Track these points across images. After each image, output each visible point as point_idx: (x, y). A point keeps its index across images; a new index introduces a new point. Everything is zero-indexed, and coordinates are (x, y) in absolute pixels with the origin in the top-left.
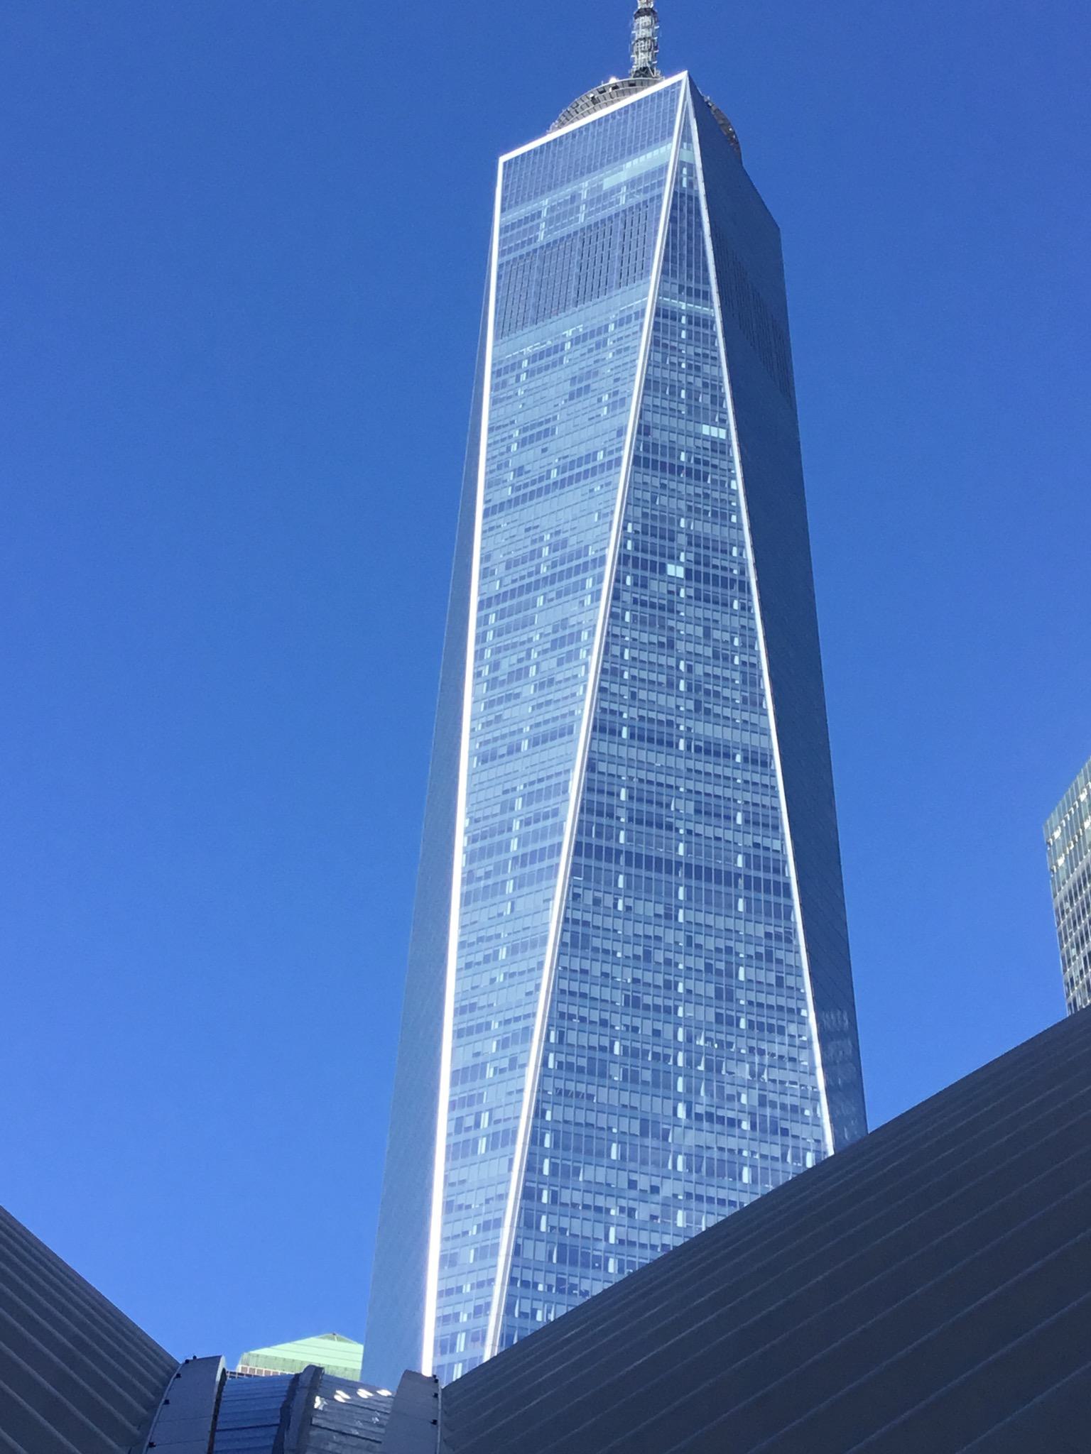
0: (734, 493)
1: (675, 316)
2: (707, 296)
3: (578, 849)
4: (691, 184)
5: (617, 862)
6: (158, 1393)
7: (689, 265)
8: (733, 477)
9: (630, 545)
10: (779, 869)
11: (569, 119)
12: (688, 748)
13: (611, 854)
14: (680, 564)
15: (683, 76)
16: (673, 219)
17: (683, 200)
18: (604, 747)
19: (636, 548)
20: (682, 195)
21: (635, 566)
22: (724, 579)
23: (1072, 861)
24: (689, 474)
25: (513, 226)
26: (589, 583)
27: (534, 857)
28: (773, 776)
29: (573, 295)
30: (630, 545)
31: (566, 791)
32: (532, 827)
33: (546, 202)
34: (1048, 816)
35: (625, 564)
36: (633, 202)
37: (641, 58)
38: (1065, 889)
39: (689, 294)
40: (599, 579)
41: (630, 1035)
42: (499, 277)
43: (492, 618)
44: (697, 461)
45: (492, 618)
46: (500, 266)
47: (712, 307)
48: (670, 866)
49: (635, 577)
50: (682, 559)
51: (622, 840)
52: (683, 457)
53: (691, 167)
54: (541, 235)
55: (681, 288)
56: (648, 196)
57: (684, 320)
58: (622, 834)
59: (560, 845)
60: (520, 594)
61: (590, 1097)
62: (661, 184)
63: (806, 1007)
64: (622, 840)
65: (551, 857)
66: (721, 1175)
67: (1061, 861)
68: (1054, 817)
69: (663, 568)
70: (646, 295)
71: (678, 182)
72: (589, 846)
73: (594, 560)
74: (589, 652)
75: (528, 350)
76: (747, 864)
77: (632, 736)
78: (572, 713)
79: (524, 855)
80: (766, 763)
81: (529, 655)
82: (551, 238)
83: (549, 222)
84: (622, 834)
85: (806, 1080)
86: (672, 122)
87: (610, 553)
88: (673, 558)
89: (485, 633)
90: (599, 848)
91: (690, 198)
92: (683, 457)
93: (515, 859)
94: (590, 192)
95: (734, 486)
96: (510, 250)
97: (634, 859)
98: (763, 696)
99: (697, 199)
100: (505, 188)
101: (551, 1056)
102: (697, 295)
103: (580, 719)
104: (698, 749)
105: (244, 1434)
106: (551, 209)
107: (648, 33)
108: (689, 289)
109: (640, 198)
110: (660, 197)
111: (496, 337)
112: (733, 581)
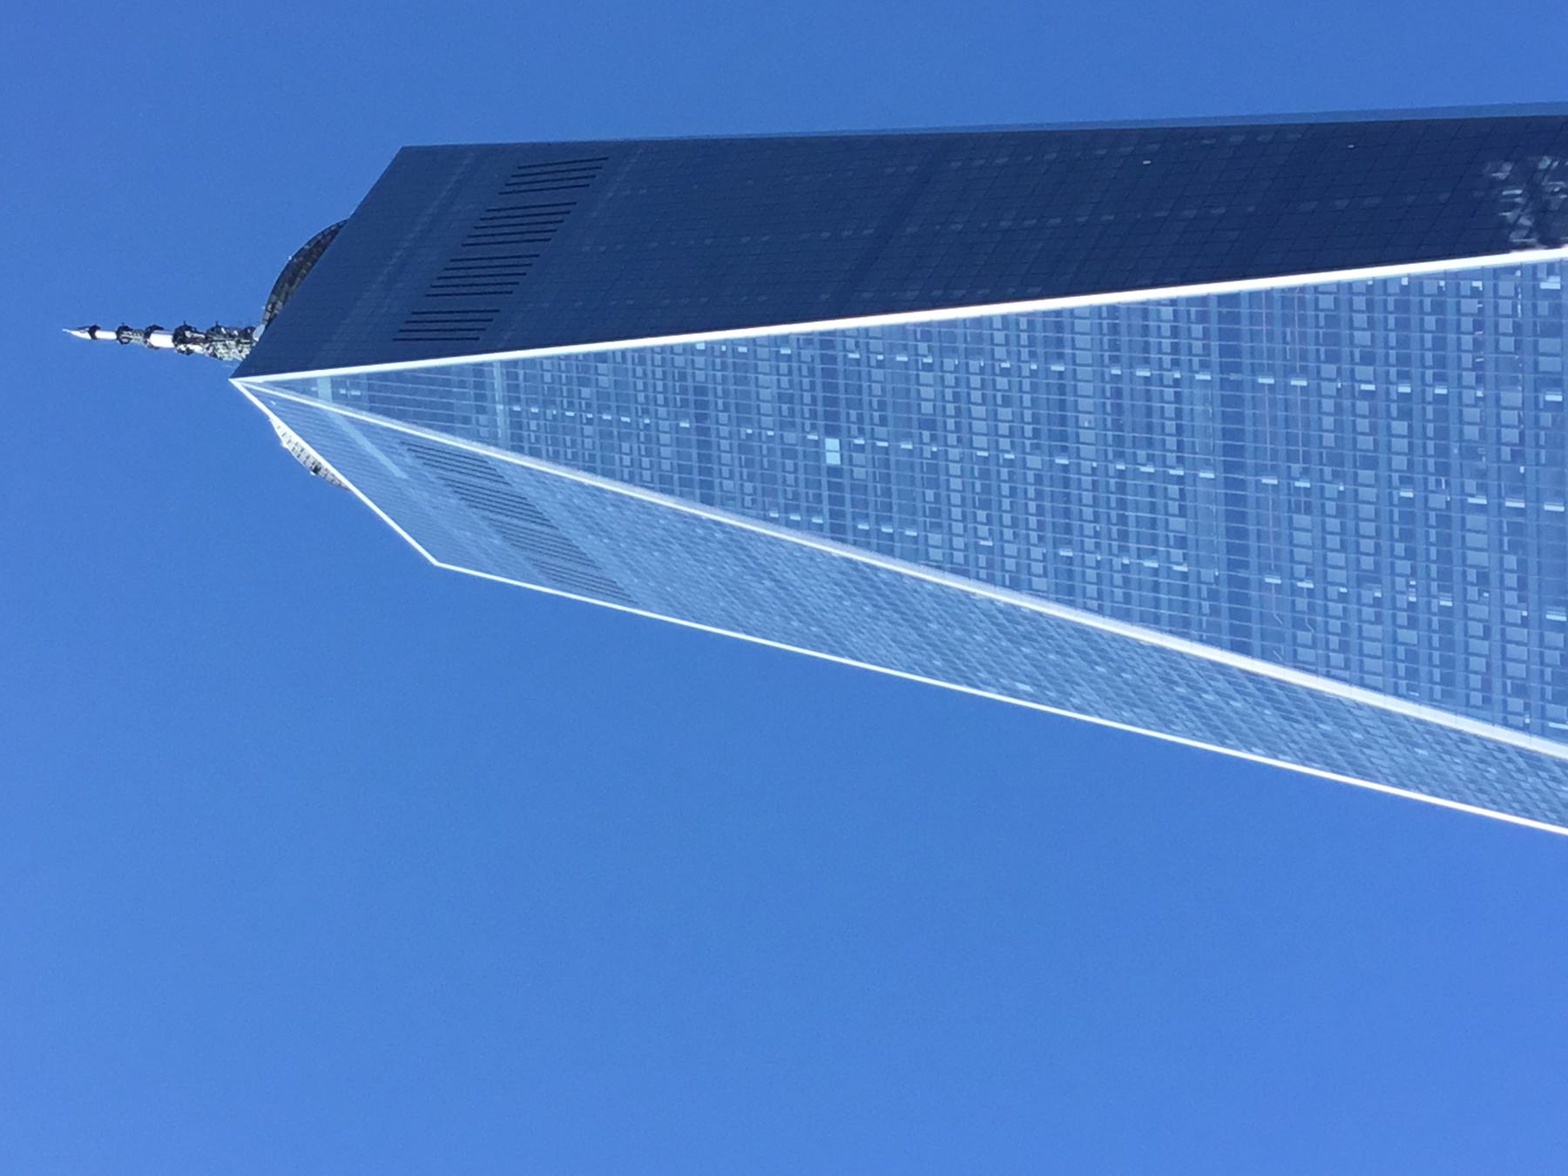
1: (516, 423)
2: (478, 369)
9: (817, 520)
17: (379, 397)
19: (819, 513)
30: (817, 520)
47: (490, 364)
53: (336, 382)
57: (517, 408)
63: (1399, 279)
69: (834, 471)
85: (1506, 287)
88: (818, 451)
95: (701, 347)
99: (370, 376)
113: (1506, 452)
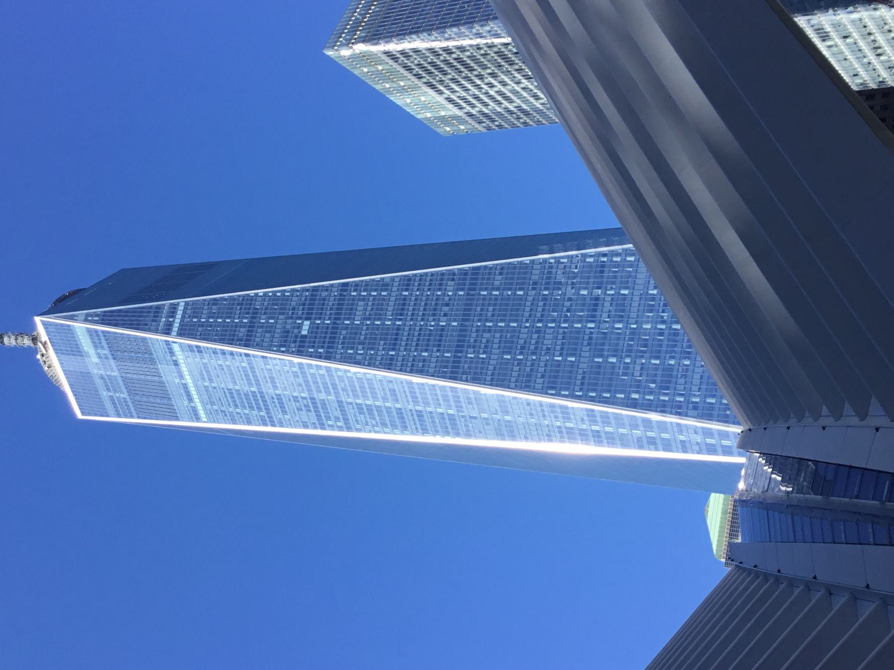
0: (265, 294)
2: (158, 307)
3: (454, 378)
4: (97, 315)
5: (460, 357)
6: (750, 572)
7: (141, 316)
8: (256, 294)
10: (465, 273)
11: (57, 381)
12: (400, 320)
13: (457, 361)
14: (302, 323)
15: (38, 320)
16: (116, 325)
17: (105, 320)
18: (399, 364)
20: (103, 320)
21: (303, 346)
22: (311, 300)
23: (465, 122)
24: (254, 318)
25: (117, 411)
26: (312, 371)
27: (457, 401)
28: (415, 275)
29: (156, 378)
31: (423, 384)
32: (441, 402)
33: (104, 394)
34: (438, 133)
35: (302, 352)
36: (106, 346)
37: (27, 342)
38: (477, 126)
39: (156, 317)
40: (310, 366)
41: (552, 352)
42: (145, 418)
43: (330, 423)
44: (248, 313)
45: (330, 423)
46: (139, 417)
48: (463, 329)
49: (309, 347)
50: (299, 321)
51: (449, 355)
52: (245, 321)
53: (87, 315)
54: (122, 396)
55: (154, 321)
56: (102, 338)
58: (446, 355)
59: (451, 387)
60: (317, 407)
61: (584, 373)
62: (96, 331)
64: (449, 355)
65: (457, 392)
66: (623, 305)
67: (462, 127)
68: (439, 130)
70: (157, 340)
71: (96, 322)
72: (451, 372)
73: (300, 368)
74: (349, 371)
75: (186, 402)
76: (462, 290)
77: (393, 350)
78: (381, 381)
79: (456, 406)
80: (409, 279)
81: (351, 403)
82: (125, 391)
83: (115, 391)
84: (446, 355)
86: (62, 325)
87: (296, 360)
88: (300, 327)
89: (338, 427)
90: (453, 367)
91: (104, 316)
92: (245, 321)
93: (458, 411)
94: (99, 369)
95: (261, 294)
96: (130, 412)
97: (459, 348)
98: (373, 280)
99: (105, 312)
100: (96, 415)
101: (563, 393)
102: (158, 312)
103: (384, 377)
104: (401, 315)
105: (771, 522)
106: (108, 390)
107: (13, 337)
108: (154, 316)
109: (104, 343)
110: (103, 332)
111: (177, 419)
112: (312, 295)
113: (565, 309)
